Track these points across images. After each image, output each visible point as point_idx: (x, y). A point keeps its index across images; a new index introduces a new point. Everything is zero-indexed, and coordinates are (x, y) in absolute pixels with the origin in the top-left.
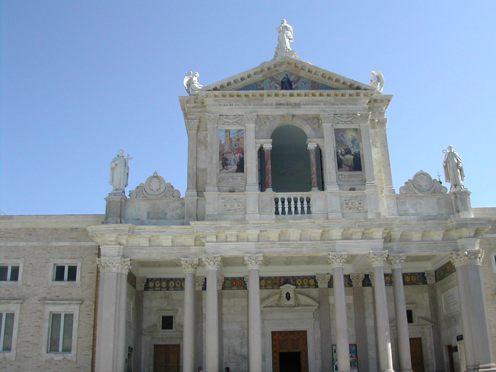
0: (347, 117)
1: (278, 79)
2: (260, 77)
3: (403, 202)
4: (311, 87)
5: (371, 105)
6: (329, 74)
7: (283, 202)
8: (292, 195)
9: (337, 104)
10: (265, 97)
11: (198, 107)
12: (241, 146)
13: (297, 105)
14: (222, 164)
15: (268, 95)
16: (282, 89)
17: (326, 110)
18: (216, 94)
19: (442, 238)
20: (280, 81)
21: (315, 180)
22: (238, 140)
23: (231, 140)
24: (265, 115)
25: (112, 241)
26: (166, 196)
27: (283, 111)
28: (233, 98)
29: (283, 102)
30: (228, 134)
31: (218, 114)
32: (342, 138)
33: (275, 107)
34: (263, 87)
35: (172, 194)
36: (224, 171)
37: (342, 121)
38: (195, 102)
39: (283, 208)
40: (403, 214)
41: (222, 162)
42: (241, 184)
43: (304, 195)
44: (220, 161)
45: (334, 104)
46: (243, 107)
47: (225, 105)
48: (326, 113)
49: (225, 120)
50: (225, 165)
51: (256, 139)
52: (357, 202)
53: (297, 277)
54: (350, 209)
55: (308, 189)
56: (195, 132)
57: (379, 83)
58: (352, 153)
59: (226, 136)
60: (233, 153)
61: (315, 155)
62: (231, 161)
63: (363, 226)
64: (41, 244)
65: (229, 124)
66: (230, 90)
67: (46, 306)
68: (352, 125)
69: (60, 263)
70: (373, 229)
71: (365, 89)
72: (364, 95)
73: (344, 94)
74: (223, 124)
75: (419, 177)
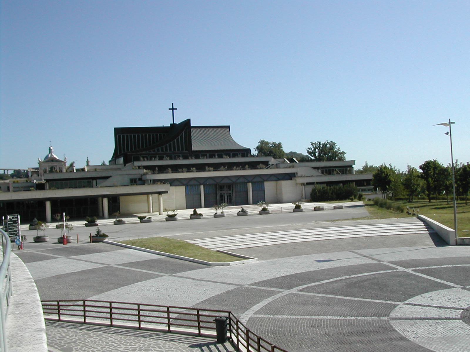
13: (53, 164)
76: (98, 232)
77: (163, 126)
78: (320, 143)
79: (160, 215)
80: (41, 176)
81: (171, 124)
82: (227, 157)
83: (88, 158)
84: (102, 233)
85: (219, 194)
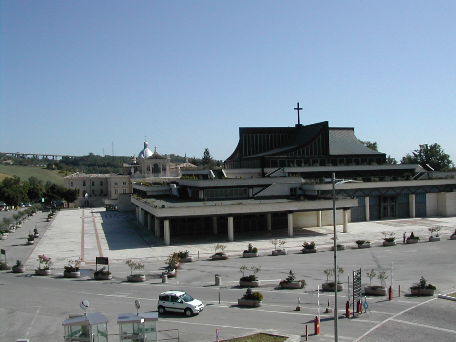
27: (155, 162)
55: (158, 173)
69: (123, 182)
76: (423, 282)
77: (288, 127)
78: (427, 145)
79: (344, 232)
80: (144, 173)
81: (296, 125)
82: (375, 165)
83: (186, 154)
84: (427, 284)
85: (383, 206)
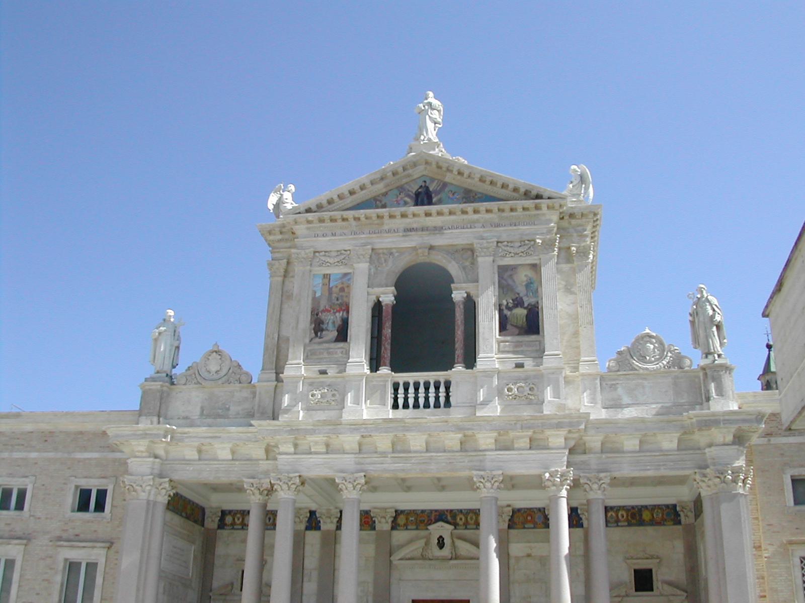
0: (520, 246)
1: (410, 189)
2: (380, 188)
3: (613, 384)
4: (463, 198)
5: (565, 223)
6: (491, 176)
7: (437, 388)
8: (421, 377)
9: (503, 225)
10: (386, 220)
11: (287, 240)
12: (345, 299)
13: (438, 230)
14: (314, 329)
15: (391, 217)
16: (416, 204)
17: (485, 235)
18: (310, 219)
19: (678, 446)
20: (412, 193)
21: (459, 351)
22: (342, 290)
23: (330, 289)
24: (386, 249)
25: (142, 452)
26: (230, 381)
28: (336, 223)
29: (415, 226)
30: (326, 281)
31: (312, 250)
32: (510, 282)
33: (401, 234)
34: (385, 203)
35: (239, 379)
36: (317, 340)
37: (510, 253)
38: (281, 233)
39: (437, 398)
40: (612, 405)
41: (315, 325)
42: (341, 360)
43: (441, 376)
44: (311, 323)
45: (498, 226)
46: (351, 237)
47: (325, 235)
48: (485, 241)
49: (323, 258)
50: (319, 331)
51: (368, 287)
52: (527, 386)
53: (458, 510)
54: (515, 399)
56: (280, 279)
57: (584, 186)
58: (526, 305)
59: (324, 284)
60: (332, 311)
61: (463, 311)
62: (328, 323)
63: (529, 428)
64: (59, 455)
65: (329, 265)
66: (333, 211)
67: (59, 549)
68: (527, 258)
69: (85, 484)
70: (548, 432)
71: (549, 198)
72: (548, 207)
73: (514, 207)
74: (320, 266)
75: (641, 342)
